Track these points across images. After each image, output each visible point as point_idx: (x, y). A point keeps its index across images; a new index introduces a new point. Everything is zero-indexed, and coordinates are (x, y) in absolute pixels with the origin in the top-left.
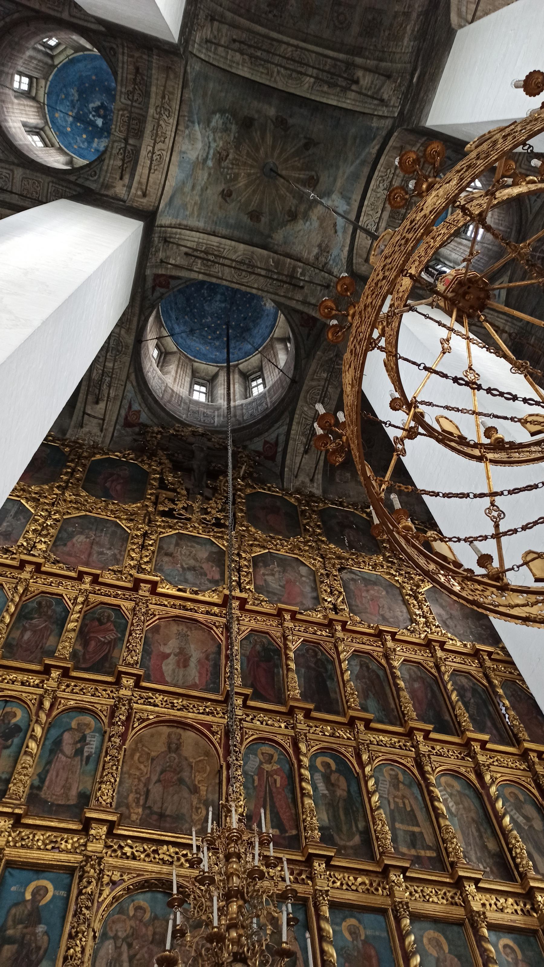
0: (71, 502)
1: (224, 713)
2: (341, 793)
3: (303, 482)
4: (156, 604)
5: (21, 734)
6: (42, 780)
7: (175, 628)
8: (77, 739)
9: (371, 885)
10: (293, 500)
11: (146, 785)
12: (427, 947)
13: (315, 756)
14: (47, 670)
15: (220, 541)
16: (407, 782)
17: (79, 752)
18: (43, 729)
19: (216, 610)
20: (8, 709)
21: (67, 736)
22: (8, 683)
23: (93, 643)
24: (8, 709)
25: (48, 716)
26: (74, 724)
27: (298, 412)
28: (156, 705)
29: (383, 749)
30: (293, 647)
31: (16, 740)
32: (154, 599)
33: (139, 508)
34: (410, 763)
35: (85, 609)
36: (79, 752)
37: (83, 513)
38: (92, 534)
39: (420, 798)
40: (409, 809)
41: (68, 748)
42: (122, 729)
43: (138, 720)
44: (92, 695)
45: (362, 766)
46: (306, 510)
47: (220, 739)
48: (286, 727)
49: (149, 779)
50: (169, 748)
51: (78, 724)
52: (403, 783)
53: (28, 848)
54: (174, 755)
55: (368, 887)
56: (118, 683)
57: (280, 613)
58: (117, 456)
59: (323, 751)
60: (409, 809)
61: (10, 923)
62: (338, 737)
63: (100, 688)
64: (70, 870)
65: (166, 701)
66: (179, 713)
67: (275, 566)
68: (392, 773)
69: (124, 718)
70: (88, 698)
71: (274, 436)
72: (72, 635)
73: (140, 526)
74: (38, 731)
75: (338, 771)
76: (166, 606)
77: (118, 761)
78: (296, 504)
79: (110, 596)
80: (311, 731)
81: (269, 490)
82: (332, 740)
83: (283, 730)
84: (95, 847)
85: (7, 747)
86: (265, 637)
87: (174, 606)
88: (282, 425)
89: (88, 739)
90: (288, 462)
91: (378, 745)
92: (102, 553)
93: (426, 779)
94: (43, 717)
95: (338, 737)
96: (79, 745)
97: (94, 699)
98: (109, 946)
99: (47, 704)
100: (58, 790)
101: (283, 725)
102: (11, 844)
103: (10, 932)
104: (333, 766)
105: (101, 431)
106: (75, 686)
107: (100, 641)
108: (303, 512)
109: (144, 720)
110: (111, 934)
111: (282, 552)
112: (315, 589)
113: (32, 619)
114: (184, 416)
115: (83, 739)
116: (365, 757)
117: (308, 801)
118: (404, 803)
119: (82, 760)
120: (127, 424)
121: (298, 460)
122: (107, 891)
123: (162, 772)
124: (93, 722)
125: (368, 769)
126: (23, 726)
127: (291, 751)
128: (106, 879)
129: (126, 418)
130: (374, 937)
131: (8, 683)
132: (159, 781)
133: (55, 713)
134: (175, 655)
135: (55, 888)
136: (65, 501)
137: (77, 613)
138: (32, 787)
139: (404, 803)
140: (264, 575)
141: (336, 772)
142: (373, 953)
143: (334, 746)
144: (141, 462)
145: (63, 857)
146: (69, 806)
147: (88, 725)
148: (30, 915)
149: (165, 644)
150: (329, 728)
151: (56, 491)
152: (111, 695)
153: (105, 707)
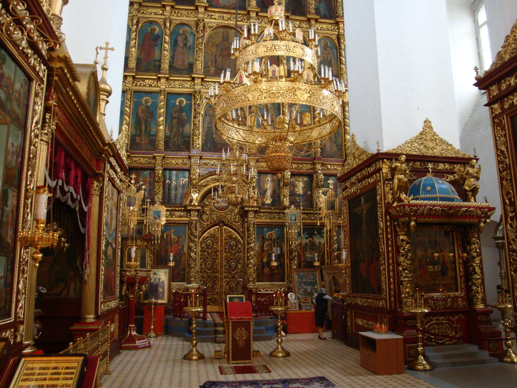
5: (161, 39)
6: (173, 60)
11: (215, 57)
14: (164, 6)
16: (331, 47)
17: (185, 45)
20: (152, 27)
24: (152, 27)
25: (169, 30)
26: (181, 31)
28: (215, 19)
29: (323, 32)
31: (159, 42)
34: (334, 37)
36: (185, 45)
39: (336, 54)
40: (329, 59)
41: (181, 44)
42: (202, 34)
49: (216, 55)
50: (223, 39)
51: (183, 31)
52: (329, 47)
53: (173, 87)
54: (226, 42)
56: (197, 9)
60: (329, 59)
61: (173, 112)
63: (190, 12)
64: (190, 94)
66: (226, 22)
68: (325, 42)
69: (201, 29)
70: (185, 18)
74: (167, 38)
77: (202, 50)
84: (197, 88)
85: (156, 46)
89: (188, 38)
93: (340, 46)
96: (185, 42)
97: (188, 19)
98: (208, 118)
100: (180, 63)
103: (174, 115)
109: (211, 27)
110: (208, 114)
115: (186, 38)
118: (327, 57)
122: (204, 101)
123: (221, 51)
124: (189, 30)
126: (160, 34)
128: (203, 97)
132: (220, 55)
133: (172, 28)
135: (186, 100)
138: (170, 62)
139: (327, 57)
145: (187, 90)
146: (185, 69)
147: (187, 31)
148: (179, 110)
150: (298, 23)
152: (195, 15)
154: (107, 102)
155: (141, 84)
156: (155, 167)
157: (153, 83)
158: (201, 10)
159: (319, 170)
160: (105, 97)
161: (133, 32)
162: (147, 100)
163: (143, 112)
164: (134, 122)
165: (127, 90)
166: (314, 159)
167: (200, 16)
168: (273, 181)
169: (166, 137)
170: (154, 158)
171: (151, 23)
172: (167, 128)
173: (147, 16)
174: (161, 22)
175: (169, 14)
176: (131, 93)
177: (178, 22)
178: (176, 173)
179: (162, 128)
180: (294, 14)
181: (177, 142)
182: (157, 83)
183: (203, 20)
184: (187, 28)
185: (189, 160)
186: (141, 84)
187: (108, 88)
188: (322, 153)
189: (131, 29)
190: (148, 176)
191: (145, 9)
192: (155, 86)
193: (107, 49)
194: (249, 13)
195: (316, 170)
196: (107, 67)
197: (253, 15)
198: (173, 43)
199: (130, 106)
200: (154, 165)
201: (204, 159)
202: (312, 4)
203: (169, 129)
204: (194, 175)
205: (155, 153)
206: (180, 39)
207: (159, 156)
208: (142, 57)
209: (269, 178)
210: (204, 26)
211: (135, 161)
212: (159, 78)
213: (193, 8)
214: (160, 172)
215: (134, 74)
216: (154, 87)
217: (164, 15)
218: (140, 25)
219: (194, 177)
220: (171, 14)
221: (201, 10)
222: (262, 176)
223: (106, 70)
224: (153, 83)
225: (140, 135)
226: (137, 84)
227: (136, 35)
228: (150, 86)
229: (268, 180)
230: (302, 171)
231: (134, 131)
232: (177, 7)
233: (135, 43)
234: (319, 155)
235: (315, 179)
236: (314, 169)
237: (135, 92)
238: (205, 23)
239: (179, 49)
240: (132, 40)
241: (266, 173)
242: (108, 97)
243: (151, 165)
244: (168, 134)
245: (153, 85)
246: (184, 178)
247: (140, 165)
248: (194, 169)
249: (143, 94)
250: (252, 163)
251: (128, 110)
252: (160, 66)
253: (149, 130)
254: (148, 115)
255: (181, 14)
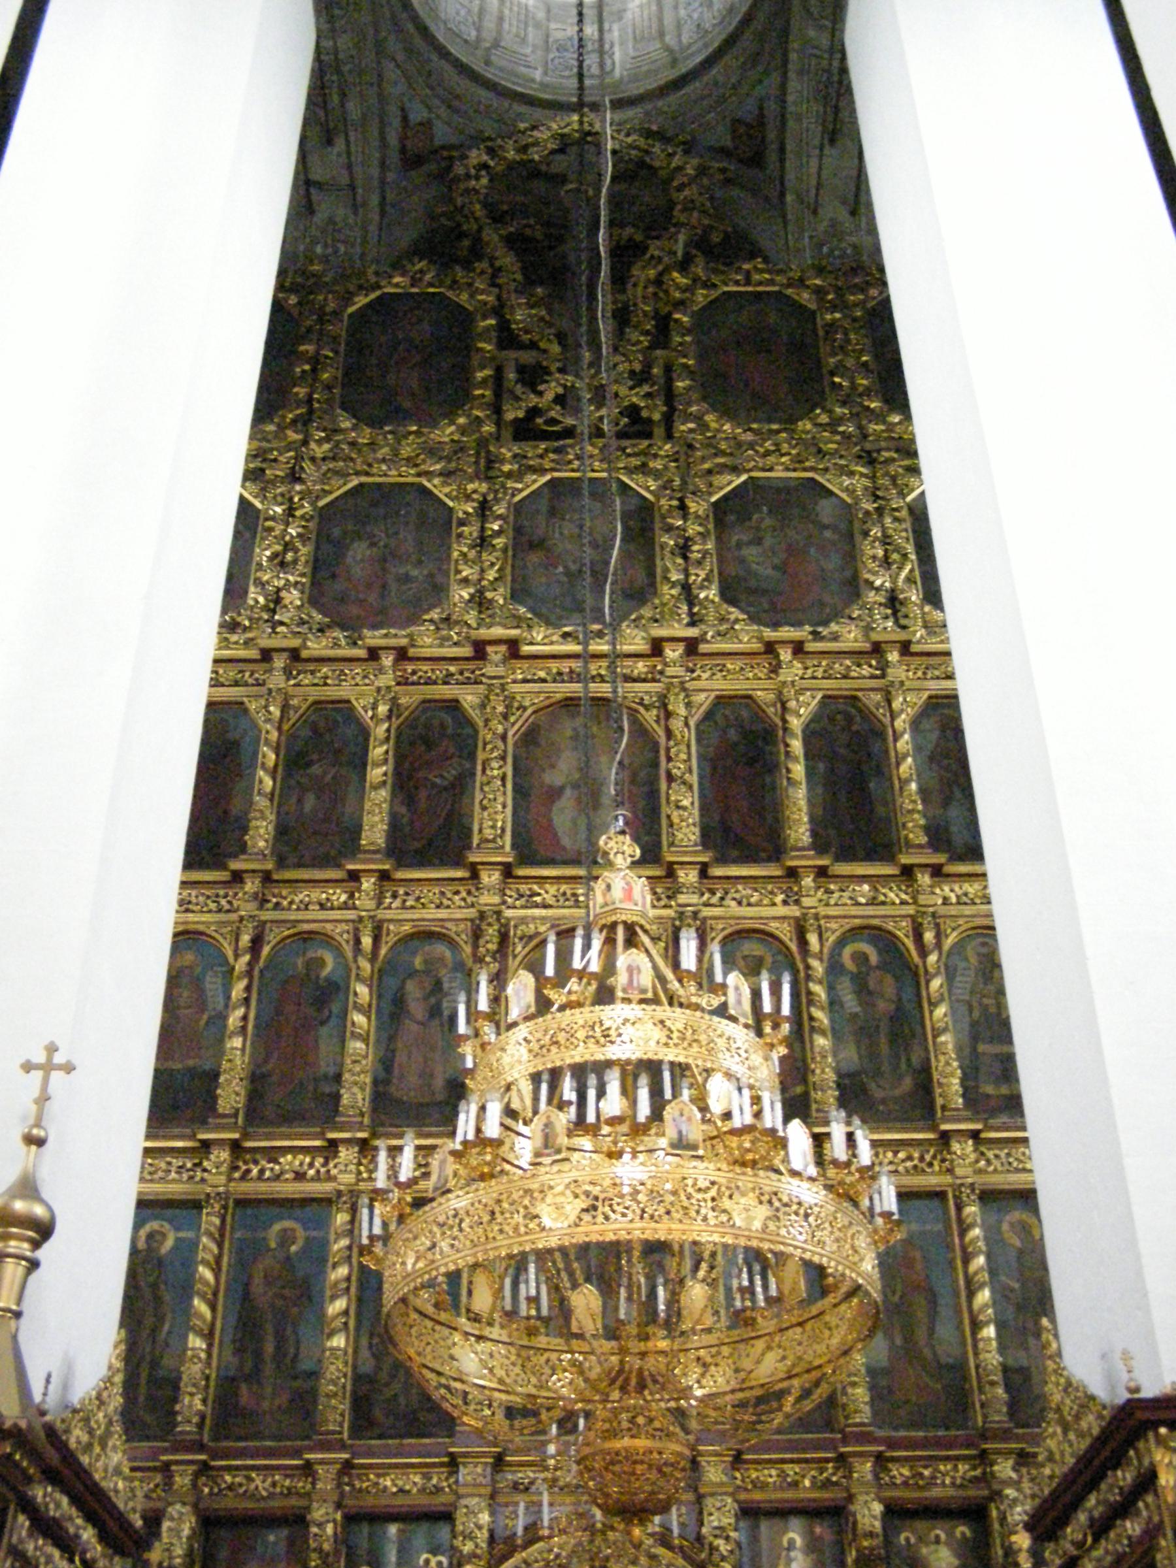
0: (324, 459)
1: (669, 897)
2: (884, 1006)
3: (834, 223)
4: (525, 681)
5: (341, 996)
7: (568, 726)
8: (429, 988)
9: (922, 1159)
10: (805, 297)
12: (1006, 1236)
13: (841, 942)
14: (354, 876)
15: (640, 478)
18: (370, 987)
19: (641, 667)
20: (311, 954)
21: (411, 986)
22: (298, 909)
23: (423, 794)
24: (311, 954)
26: (418, 962)
27: (795, 45)
28: (546, 906)
29: (968, 910)
30: (796, 723)
31: (335, 1008)
32: (520, 671)
33: (463, 431)
35: (396, 722)
37: (354, 482)
38: (378, 531)
41: (417, 1008)
43: (521, 939)
44: (438, 907)
45: (923, 952)
46: (834, 321)
47: (666, 949)
48: (785, 903)
51: (426, 962)
55: (916, 1162)
56: (475, 875)
57: (770, 648)
58: (397, 285)
59: (854, 933)
62: (883, 903)
65: (564, 894)
67: (764, 518)
69: (492, 947)
70: (432, 913)
71: (751, 105)
72: (384, 793)
73: (470, 487)
74: (362, 990)
75: (883, 966)
76: (544, 681)
78: (813, 306)
79: (435, 683)
80: (832, 902)
81: (748, 282)
82: (870, 910)
83: (781, 911)
85: (323, 1023)
86: (747, 705)
87: (559, 677)
88: (767, 72)
89: (446, 986)
90: (790, 176)
91: (959, 903)
92: (407, 579)
94: (365, 966)
95: (883, 903)
96: (433, 1000)
97: (442, 914)
99: (367, 941)
101: (780, 898)
102: (365, 1175)
104: (874, 958)
105: (355, 208)
106: (407, 894)
107: (434, 785)
108: (831, 327)
111: (779, 473)
112: (851, 556)
113: (309, 764)
114: (538, 75)
116: (929, 936)
117: (821, 1042)
119: (442, 1025)
120: (412, 161)
121: (814, 163)
125: (932, 958)
127: (793, 947)
129: (403, 150)
130: (923, 1233)
131: (298, 909)
133: (383, 951)
134: (576, 786)
136: (313, 459)
137: (381, 744)
138: (375, 1082)
140: (739, 545)
141: (878, 967)
142: (918, 1255)
143: (876, 922)
144: (451, 288)
147: (442, 959)
149: (553, 766)
151: (293, 436)
152: (470, 900)
153: (462, 926)
154: (34, 1265)
155: (262, 1171)
156: (308, 1509)
157: (311, 1165)
158: (491, 878)
159: (1009, 1483)
160: (26, 1245)
161: (239, 978)
162: (285, 1230)
163: (268, 1280)
164: (232, 1320)
165: (208, 1195)
166: (984, 1436)
167: (489, 899)
168: (813, 1546)
169: (358, 1378)
170: (308, 1469)
171: (305, 940)
172: (364, 1341)
173: (293, 916)
174: (341, 933)
175: (371, 904)
176: (225, 1207)
177: (407, 928)
178: (399, 1530)
179: (339, 1341)
180: (846, 854)
181: (402, 1400)
182: (325, 1164)
183: (498, 913)
184: (441, 949)
185: (451, 1474)
186: (262, 1171)
187: (39, 1211)
188: (1013, 1407)
189: (233, 968)
190: (282, 1548)
191: (284, 893)
192: (317, 1178)
193: (48, 1067)
194: (671, 873)
195: (996, 1487)
196: (42, 1134)
197: (688, 876)
198: (387, 1008)
199: (218, 1259)
200: (302, 1503)
201: (510, 1464)
202: (911, 812)
203: (370, 1346)
204: (469, 1536)
205: (311, 1450)
206: (413, 989)
207: (327, 1462)
208: (270, 1066)
209: (794, 1534)
210: (504, 938)
211: (230, 1487)
212: (333, 1145)
213: (460, 874)
214: (330, 1529)
215: (236, 1136)
216: (312, 1179)
217: (355, 908)
218: (266, 950)
219: (468, 1547)
220: (379, 904)
221: (491, 878)
222: (765, 1527)
223: (40, 1142)
224: (311, 1165)
225: (254, 1376)
226: (248, 1171)
227: (248, 989)
228: (300, 1176)
229: (791, 1545)
230: (936, 1492)
231: (235, 1361)
232: (400, 875)
233: (245, 1018)
234: (999, 1416)
235: (996, 1526)
236: (985, 1479)
237: (242, 1203)
238: (507, 925)
239: (411, 1028)
240: (234, 1008)
241: (782, 1513)
242: (36, 1245)
243: (294, 1501)
244: (367, 1366)
245: (312, 1172)
246: (434, 1552)
247: (250, 1505)
248: (471, 1512)
249: (275, 1210)
250: (714, 1473)
251: (208, 1275)
252: (337, 1097)
253: (292, 1350)
254: (286, 1292)
255: (418, 899)
